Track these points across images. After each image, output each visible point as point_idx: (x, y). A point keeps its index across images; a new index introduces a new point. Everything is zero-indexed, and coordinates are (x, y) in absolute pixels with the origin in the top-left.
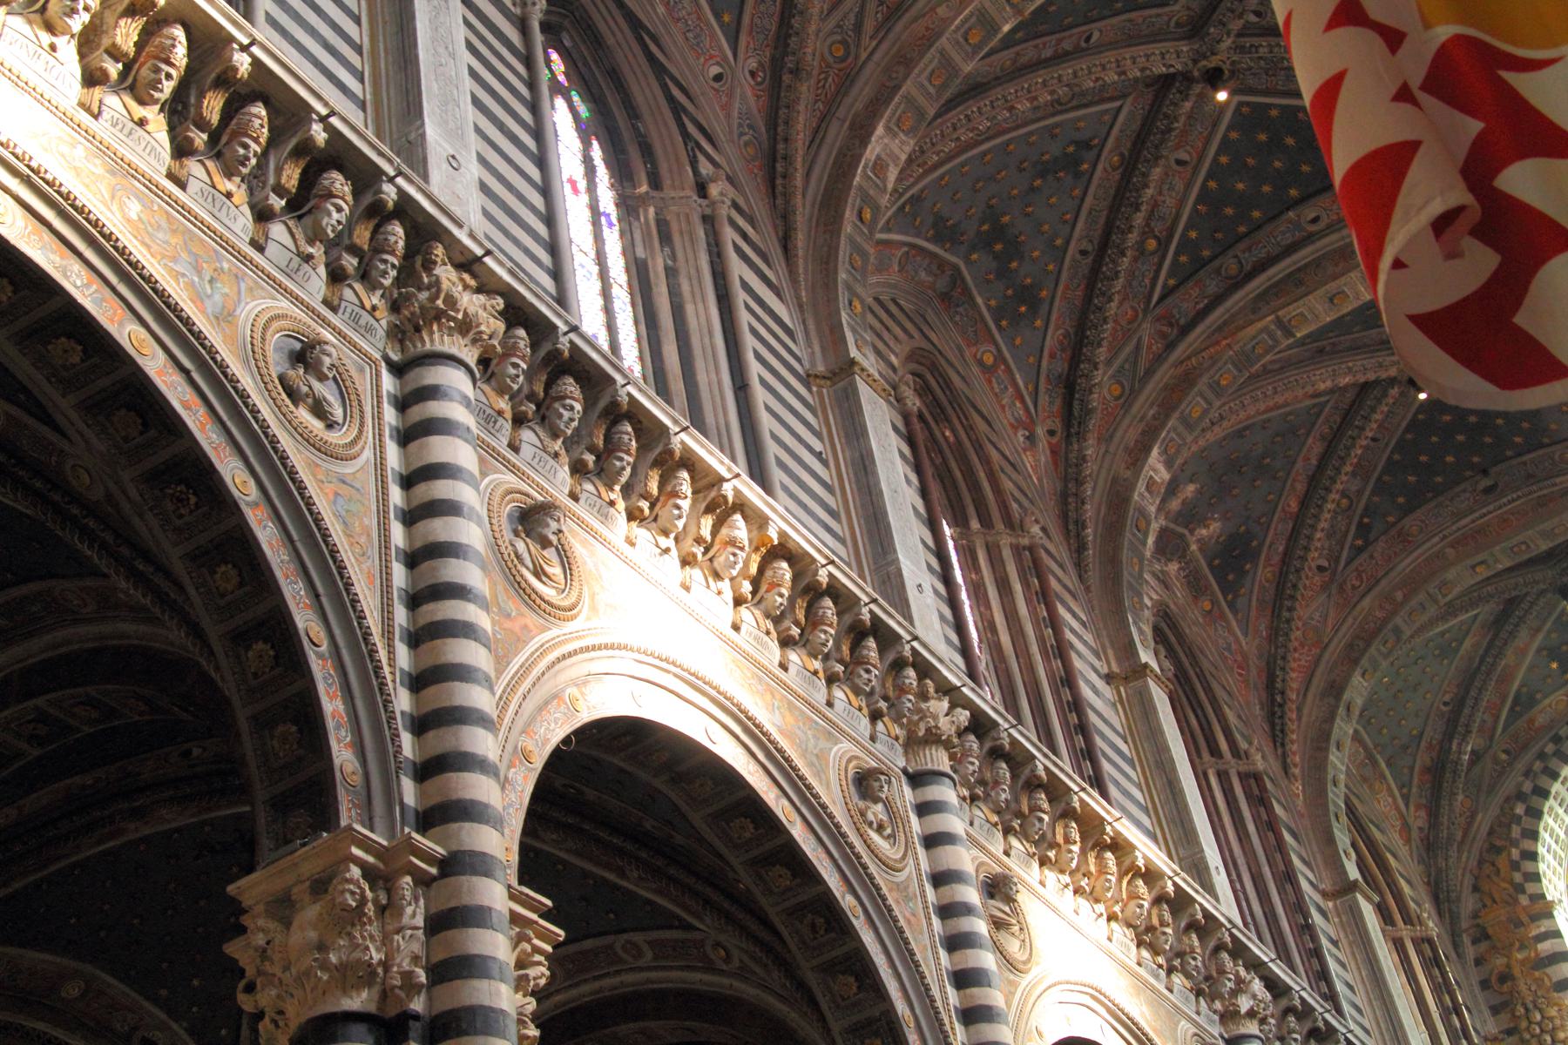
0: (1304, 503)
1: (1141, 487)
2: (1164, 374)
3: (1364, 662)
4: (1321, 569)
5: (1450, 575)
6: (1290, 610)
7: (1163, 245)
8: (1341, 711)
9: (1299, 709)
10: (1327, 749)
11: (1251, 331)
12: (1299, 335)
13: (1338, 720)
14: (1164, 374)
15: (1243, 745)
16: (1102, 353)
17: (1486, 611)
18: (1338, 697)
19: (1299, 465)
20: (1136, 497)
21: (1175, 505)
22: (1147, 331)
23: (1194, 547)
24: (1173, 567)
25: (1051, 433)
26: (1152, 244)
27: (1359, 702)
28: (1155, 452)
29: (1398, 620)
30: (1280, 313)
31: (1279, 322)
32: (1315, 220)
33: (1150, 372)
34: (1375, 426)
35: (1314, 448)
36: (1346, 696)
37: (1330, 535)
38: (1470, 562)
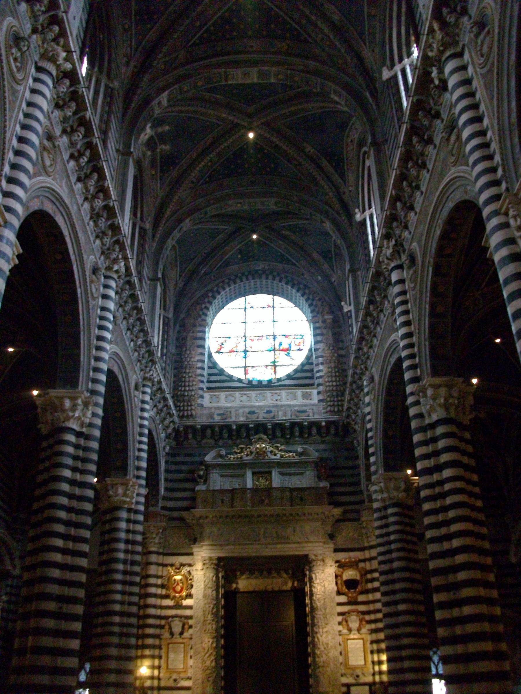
0: (199, 156)
1: (156, 101)
2: (181, 71)
3: (192, 217)
4: (192, 182)
5: (230, 202)
6: (178, 189)
7: (201, 27)
8: (179, 228)
9: (166, 223)
10: (169, 237)
11: (216, 71)
12: (229, 82)
13: (176, 231)
14: (181, 71)
15: (145, 219)
16: (165, 49)
17: (229, 228)
18: (179, 224)
19: (202, 143)
20: (153, 103)
21: (160, 130)
22: (182, 54)
23: (158, 150)
24: (149, 153)
25: (135, 67)
26: (198, 24)
27: (185, 229)
28: (166, 93)
29: (208, 209)
30: (228, 70)
31: (225, 72)
32: (252, 47)
33: (176, 68)
34: (231, 140)
35: (209, 139)
36: (182, 224)
37: (200, 172)
38: (236, 201)
